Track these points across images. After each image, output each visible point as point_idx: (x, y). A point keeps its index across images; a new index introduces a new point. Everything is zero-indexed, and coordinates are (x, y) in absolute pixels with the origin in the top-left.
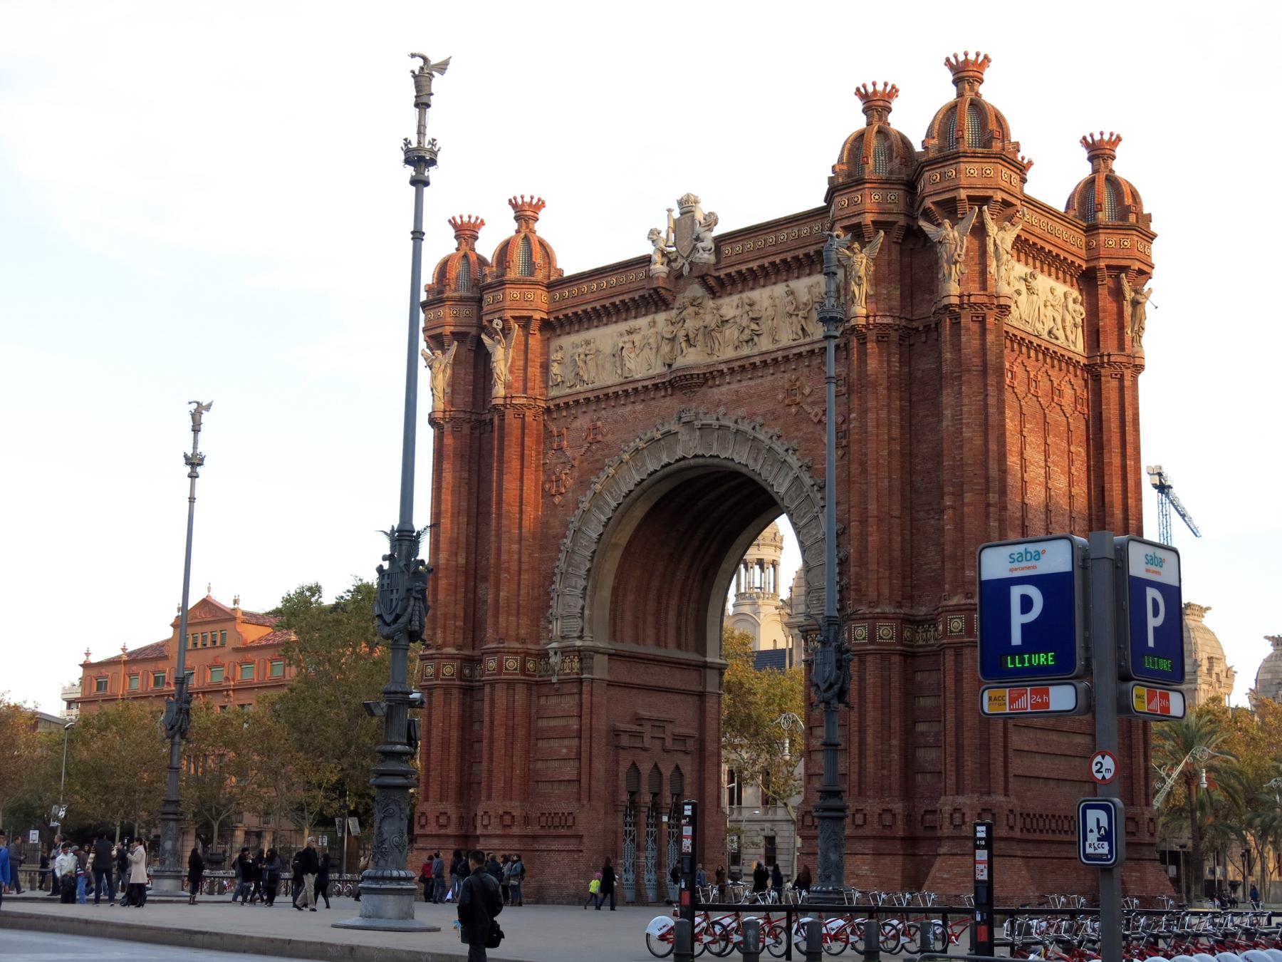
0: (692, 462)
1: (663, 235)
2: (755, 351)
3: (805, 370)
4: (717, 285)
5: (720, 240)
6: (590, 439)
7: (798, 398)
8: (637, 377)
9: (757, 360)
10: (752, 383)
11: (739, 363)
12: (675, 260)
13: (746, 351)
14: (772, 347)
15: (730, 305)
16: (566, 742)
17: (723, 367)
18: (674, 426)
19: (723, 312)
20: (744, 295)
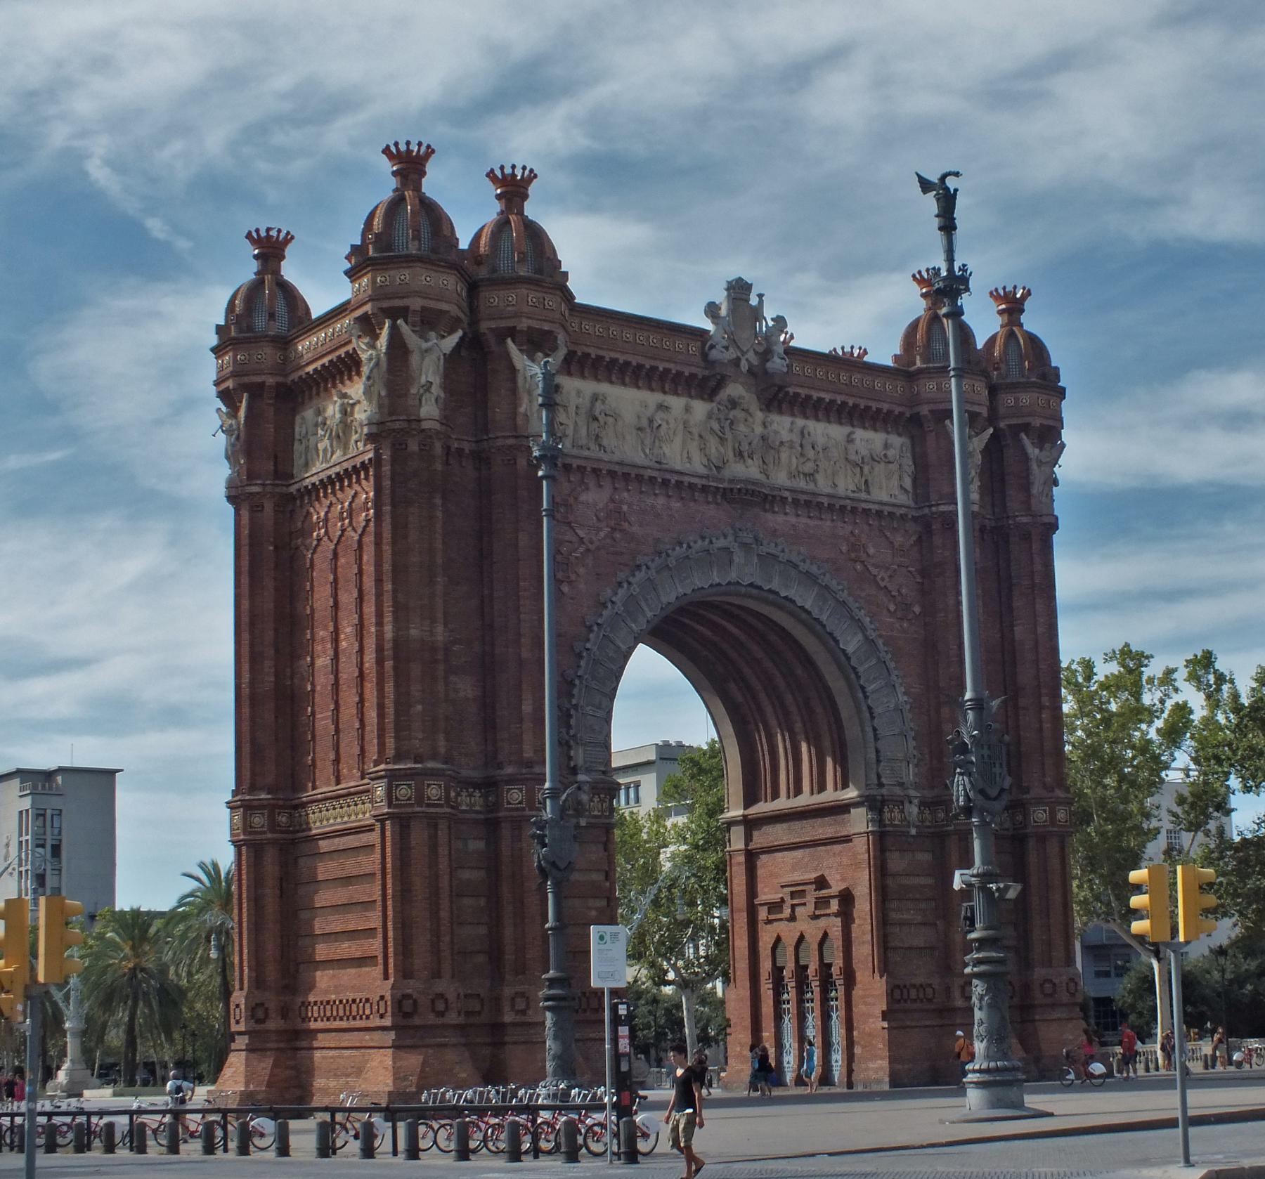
0: (743, 590)
1: (723, 312)
2: (811, 487)
3: (866, 527)
4: (777, 397)
6: (612, 523)
7: (864, 557)
8: (678, 467)
9: (825, 501)
10: (809, 521)
11: (804, 497)
13: (802, 484)
14: (829, 490)
15: (783, 425)
16: (591, 902)
17: (786, 494)
19: (775, 426)
20: (800, 422)
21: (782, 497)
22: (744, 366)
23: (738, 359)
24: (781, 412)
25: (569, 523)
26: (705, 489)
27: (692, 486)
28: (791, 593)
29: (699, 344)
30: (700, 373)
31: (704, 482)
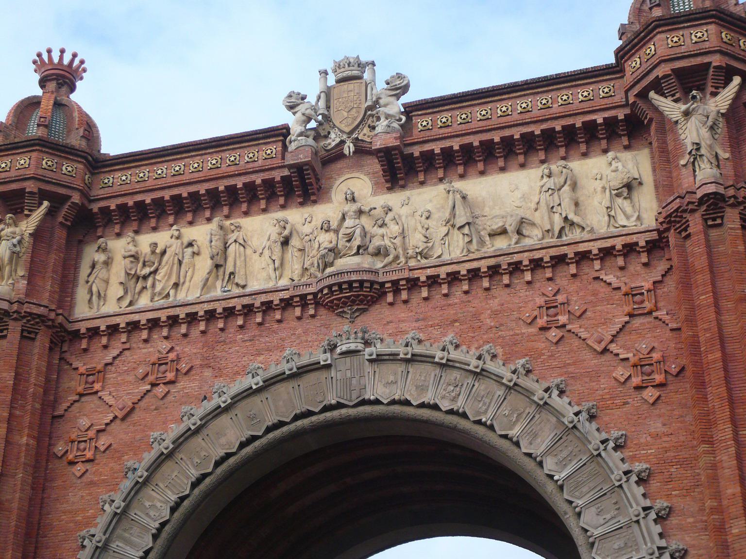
0: (352, 412)
1: (312, 99)
5: (411, 110)
6: (151, 378)
7: (563, 319)
12: (326, 137)
18: (324, 358)
21: (408, 280)
22: (349, 148)
23: (342, 142)
24: (422, 183)
25: (96, 392)
26: (287, 304)
27: (268, 307)
28: (428, 398)
29: (280, 144)
30: (277, 175)
31: (285, 295)
